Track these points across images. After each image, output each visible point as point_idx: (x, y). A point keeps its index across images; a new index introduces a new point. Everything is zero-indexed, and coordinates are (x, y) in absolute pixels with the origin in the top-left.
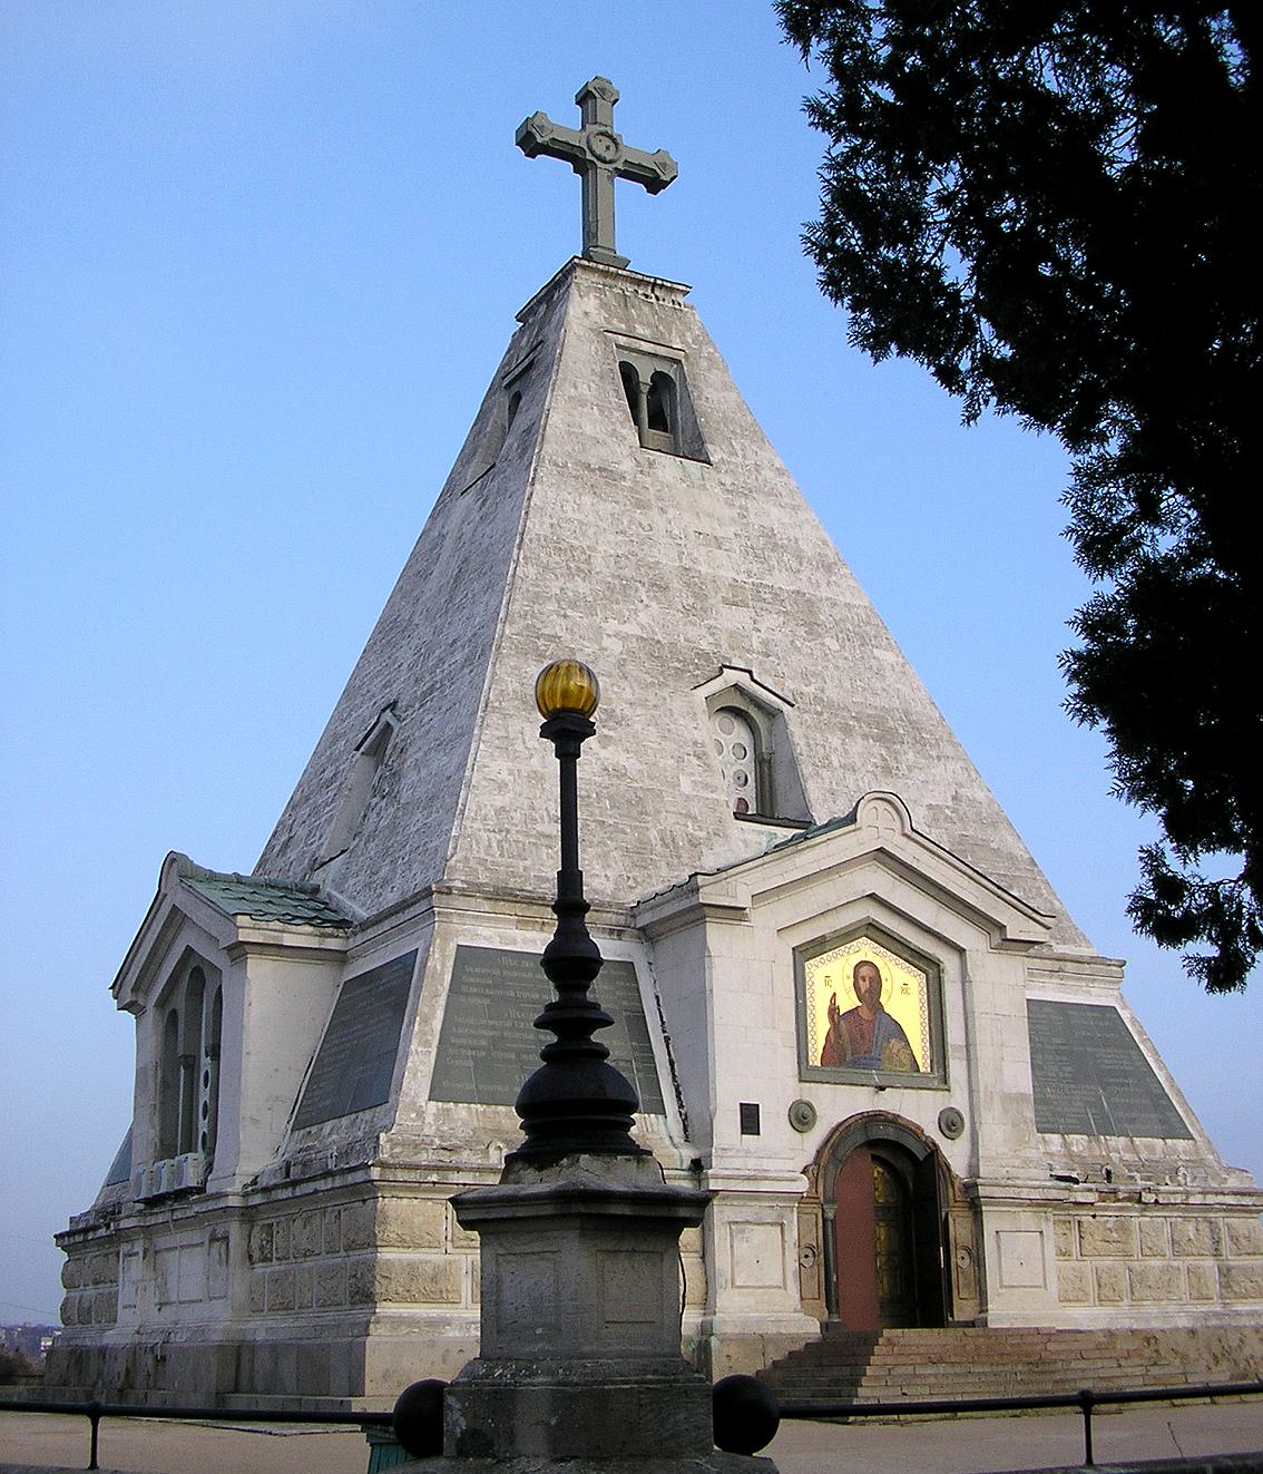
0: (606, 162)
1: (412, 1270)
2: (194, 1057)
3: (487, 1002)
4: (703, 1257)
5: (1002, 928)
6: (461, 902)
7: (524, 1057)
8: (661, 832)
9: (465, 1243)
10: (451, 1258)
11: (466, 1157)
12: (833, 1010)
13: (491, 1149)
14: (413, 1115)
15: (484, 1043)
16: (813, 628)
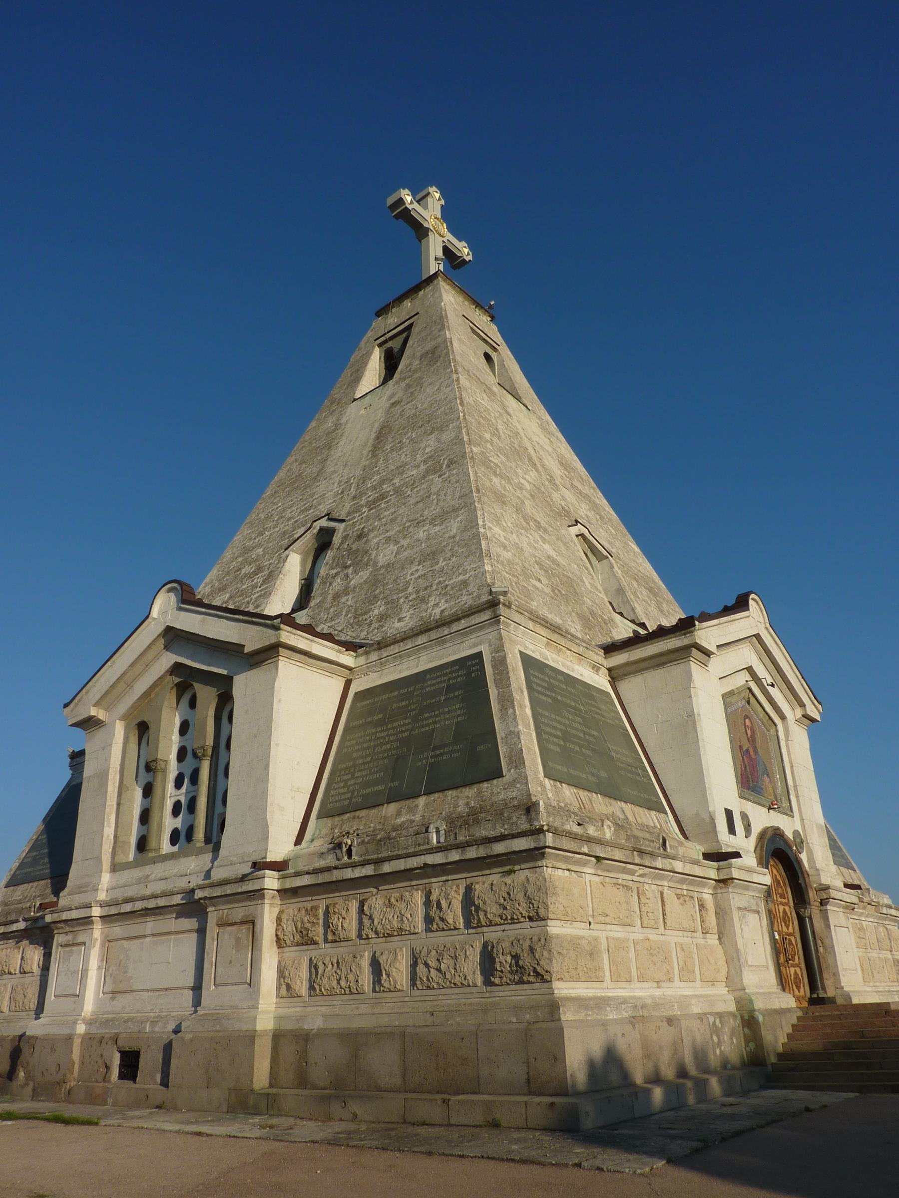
0: (440, 235)
1: (575, 943)
2: (166, 761)
3: (550, 701)
4: (720, 939)
5: (802, 705)
6: (517, 617)
7: (584, 751)
8: (588, 608)
9: (602, 919)
10: (595, 933)
11: (592, 831)
12: (741, 747)
13: (605, 827)
14: (539, 789)
15: (560, 734)
16: (601, 517)
